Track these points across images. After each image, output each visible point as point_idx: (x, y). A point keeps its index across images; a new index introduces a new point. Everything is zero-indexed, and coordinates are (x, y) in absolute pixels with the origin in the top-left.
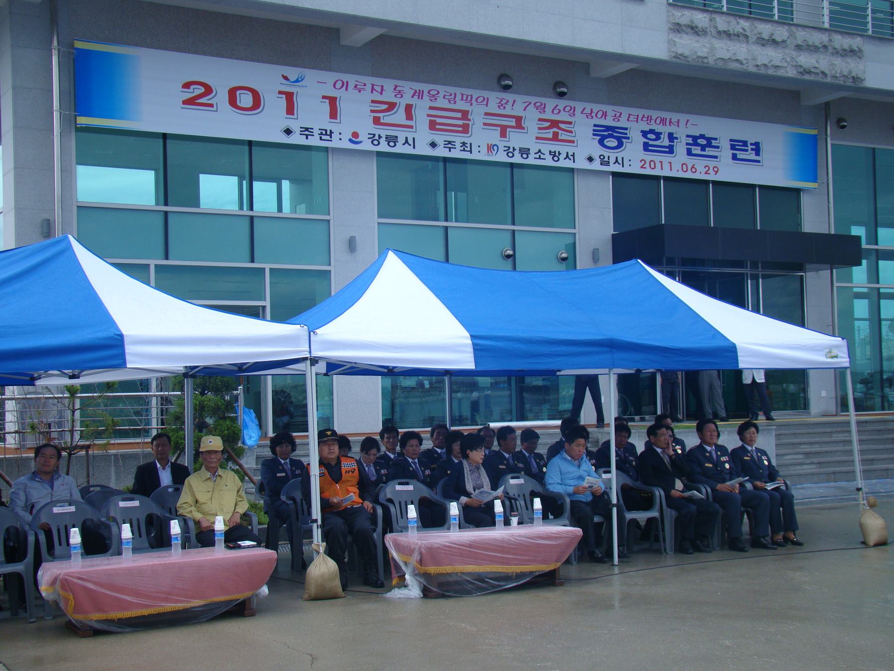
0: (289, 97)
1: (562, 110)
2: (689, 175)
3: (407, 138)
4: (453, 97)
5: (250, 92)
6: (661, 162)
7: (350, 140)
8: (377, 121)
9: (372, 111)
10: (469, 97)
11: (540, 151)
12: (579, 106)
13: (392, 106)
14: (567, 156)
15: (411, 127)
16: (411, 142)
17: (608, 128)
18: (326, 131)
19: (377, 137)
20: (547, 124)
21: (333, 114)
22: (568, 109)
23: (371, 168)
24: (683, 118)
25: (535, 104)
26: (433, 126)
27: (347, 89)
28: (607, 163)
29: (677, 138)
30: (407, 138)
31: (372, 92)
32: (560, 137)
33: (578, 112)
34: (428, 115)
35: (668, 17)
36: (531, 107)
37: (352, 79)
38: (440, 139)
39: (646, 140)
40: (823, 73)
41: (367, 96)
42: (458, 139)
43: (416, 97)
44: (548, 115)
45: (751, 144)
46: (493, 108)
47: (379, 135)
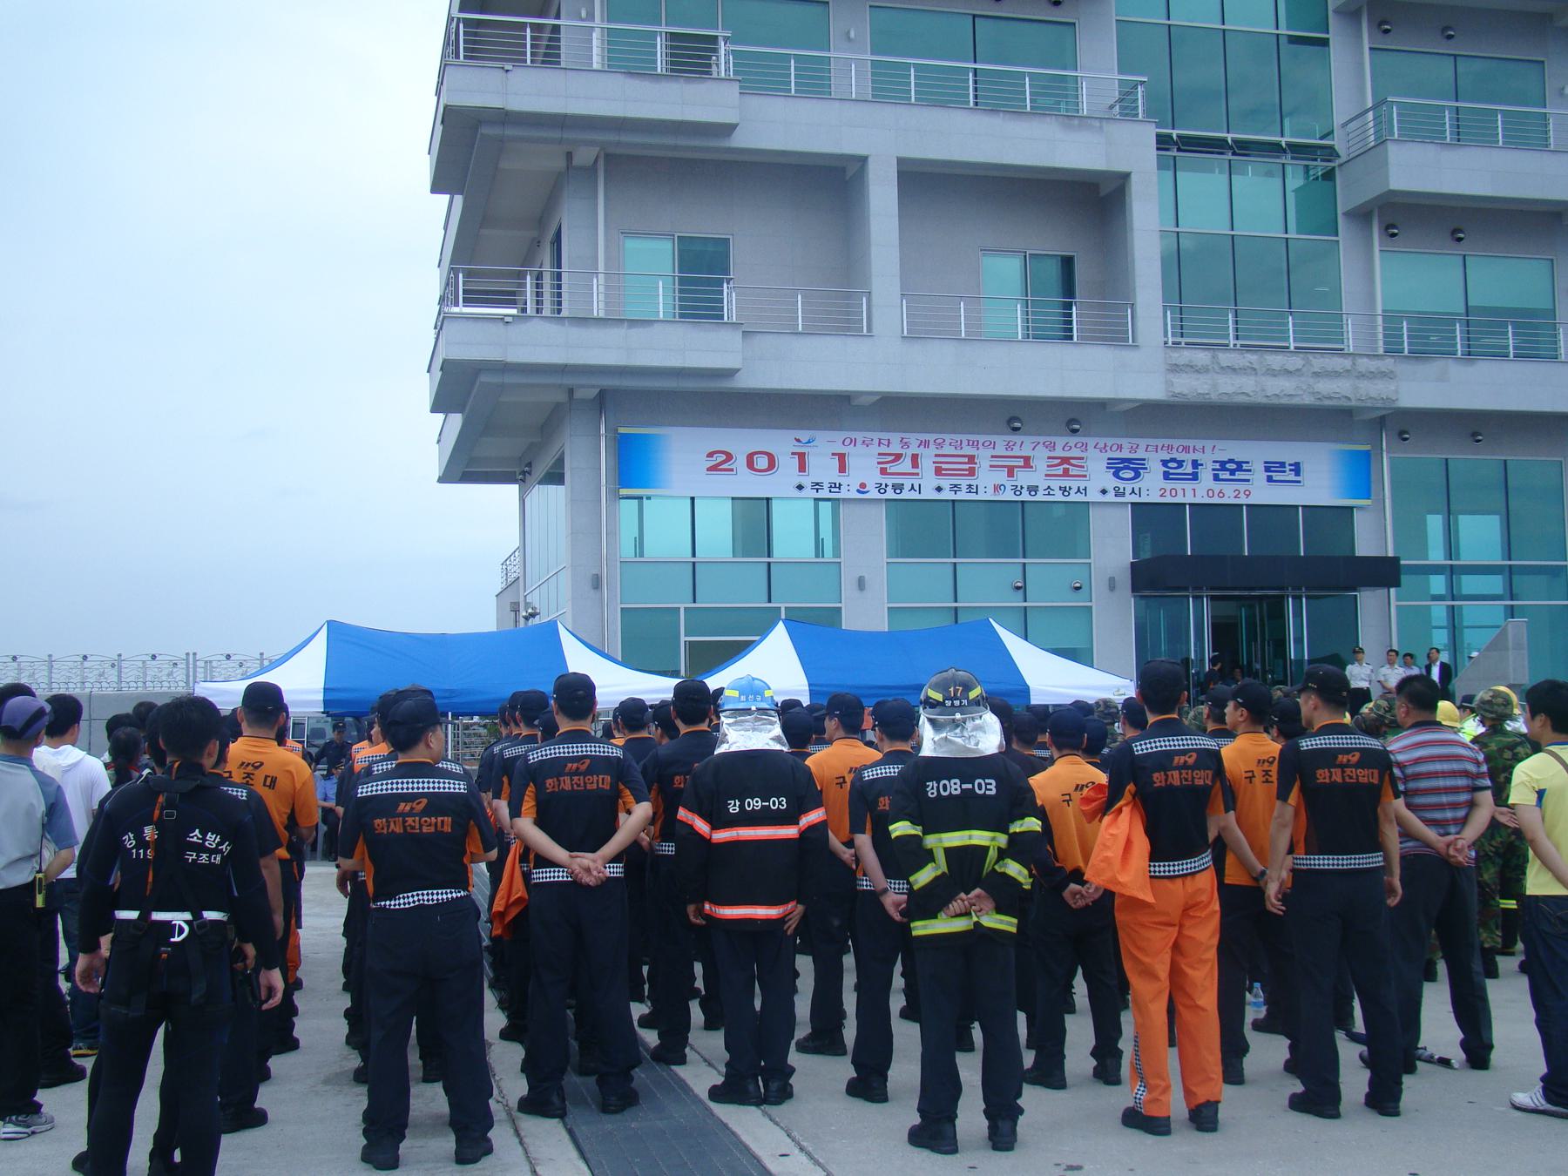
0: (801, 456)
1: (1073, 446)
3: (912, 485)
7: (858, 491)
8: (883, 472)
9: (879, 463)
10: (976, 443)
11: (1049, 487)
12: (1091, 441)
13: (898, 457)
14: (1079, 490)
16: (917, 488)
17: (1124, 460)
18: (835, 484)
19: (883, 486)
20: (1058, 461)
21: (842, 469)
24: (1209, 444)
26: (938, 472)
27: (855, 445)
28: (1123, 494)
29: (1202, 465)
30: (912, 485)
33: (1091, 447)
36: (1041, 446)
37: (859, 436)
38: (946, 483)
41: (875, 449)
43: (922, 447)
44: (1059, 453)
45: (1290, 465)
46: (1000, 451)
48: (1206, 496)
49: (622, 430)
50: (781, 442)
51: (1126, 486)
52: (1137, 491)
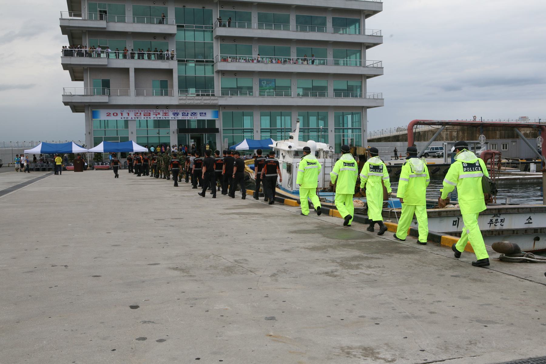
0: (122, 114)
8: (135, 115)
12: (170, 110)
13: (138, 113)
17: (175, 113)
21: (128, 115)
24: (190, 110)
26: (144, 115)
36: (161, 111)
37: (131, 110)
38: (145, 117)
41: (134, 112)
42: (148, 117)
44: (164, 112)
46: (155, 112)
49: (93, 110)
50: (118, 111)
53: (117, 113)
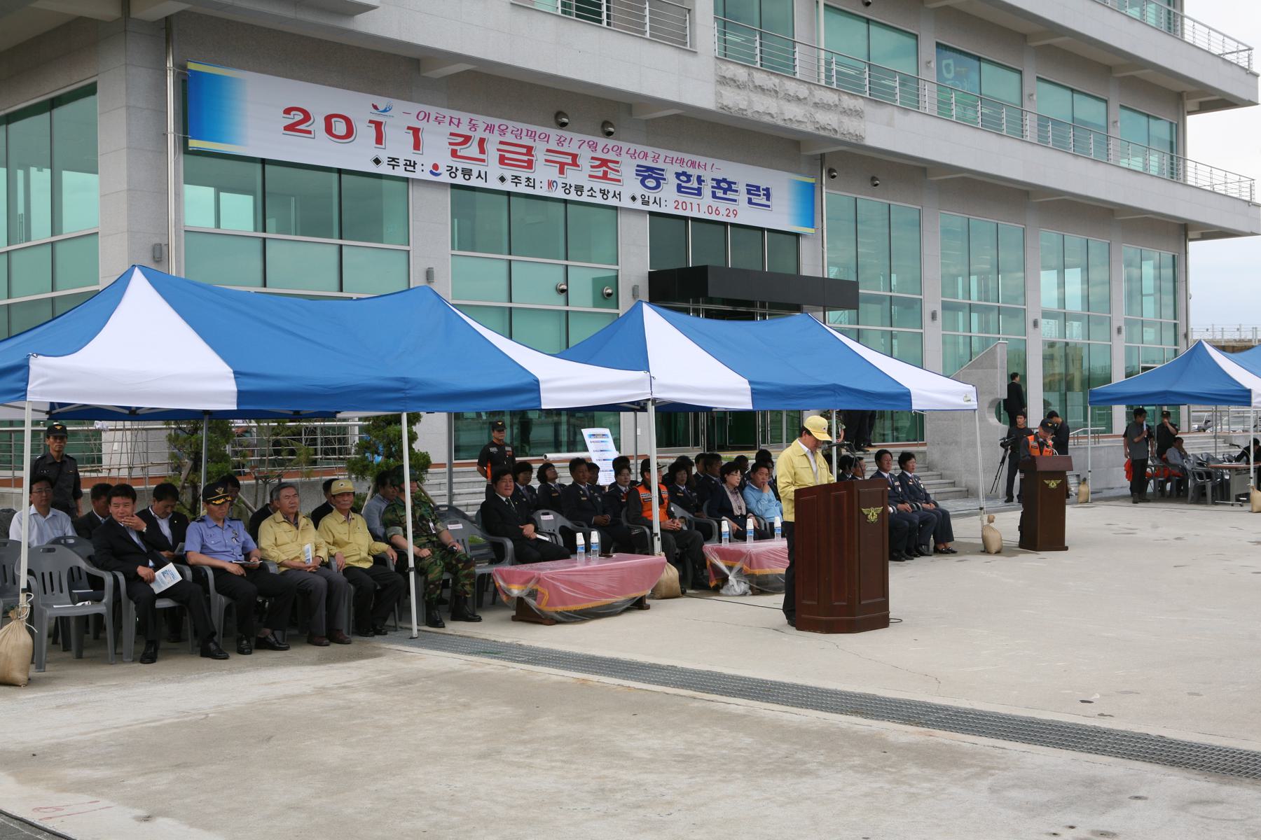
0: (378, 125)
1: (611, 150)
2: (713, 217)
4: (519, 132)
5: (345, 121)
6: (691, 204)
7: (431, 172)
8: (454, 154)
9: (450, 144)
10: (534, 133)
11: (592, 189)
12: (625, 146)
13: (467, 139)
15: (483, 161)
16: (483, 176)
18: (410, 161)
19: (454, 170)
20: (598, 163)
21: (417, 146)
22: (615, 148)
23: (446, 197)
24: (709, 161)
25: (588, 143)
26: (502, 160)
27: (428, 121)
29: (704, 181)
30: (480, 171)
31: (450, 125)
32: (609, 176)
34: (499, 150)
35: (716, 70)
38: (508, 173)
39: (680, 182)
40: (835, 130)
41: (447, 129)
42: (524, 174)
43: (487, 131)
44: (599, 154)
45: (763, 190)
46: (553, 145)
47: (456, 168)
48: (707, 211)
51: (650, 194)
52: (658, 201)
53: (345, 114)
